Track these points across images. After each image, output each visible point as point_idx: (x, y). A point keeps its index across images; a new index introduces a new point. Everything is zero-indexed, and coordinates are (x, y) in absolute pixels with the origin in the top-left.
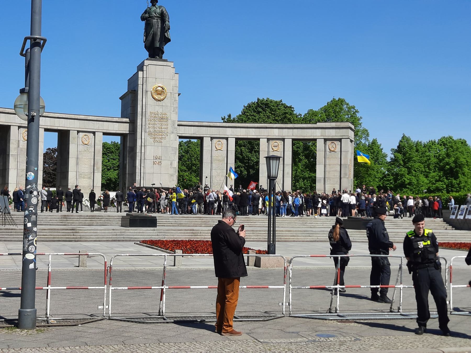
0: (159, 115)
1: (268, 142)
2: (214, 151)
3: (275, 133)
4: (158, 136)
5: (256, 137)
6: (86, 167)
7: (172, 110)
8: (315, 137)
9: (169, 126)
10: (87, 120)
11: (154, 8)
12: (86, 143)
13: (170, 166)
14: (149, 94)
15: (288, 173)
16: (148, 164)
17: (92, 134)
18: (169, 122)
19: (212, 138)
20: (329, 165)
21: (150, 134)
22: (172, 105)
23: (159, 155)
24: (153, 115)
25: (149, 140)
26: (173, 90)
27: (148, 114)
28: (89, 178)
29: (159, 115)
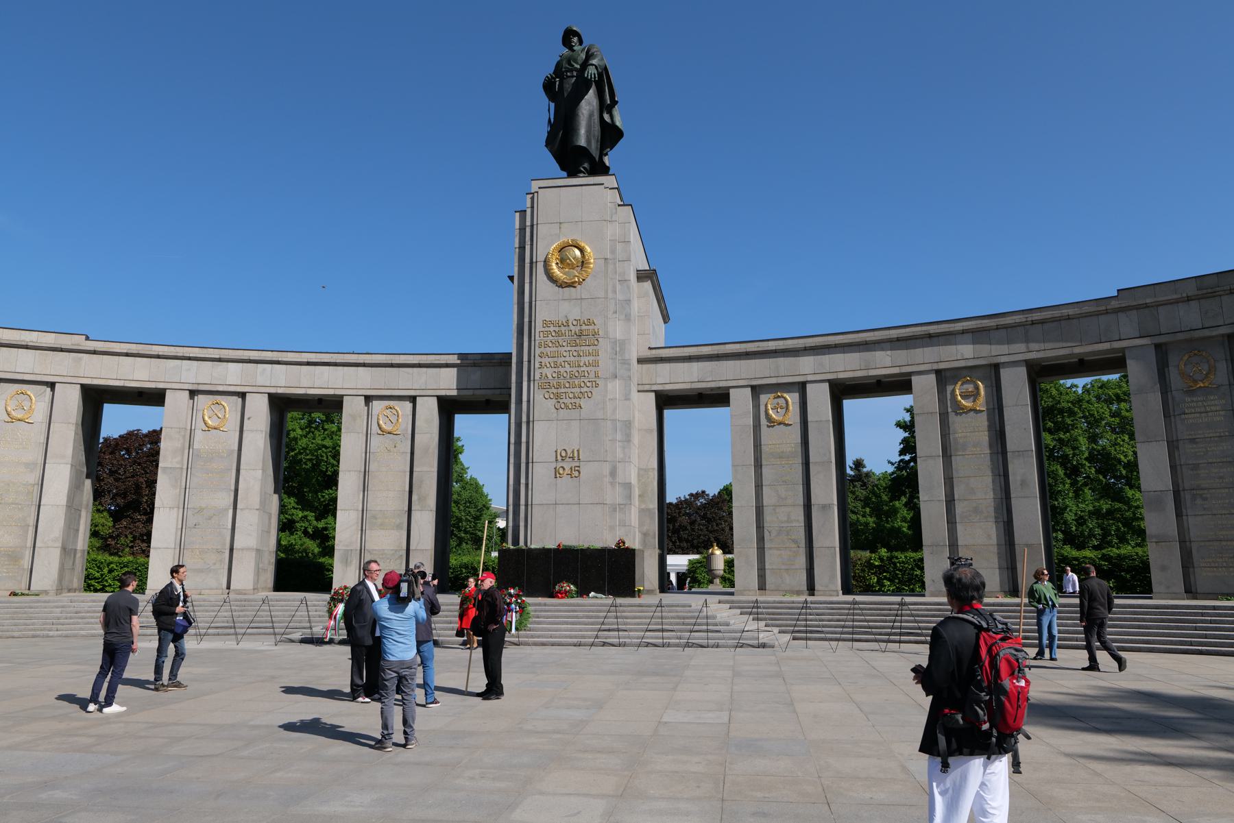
0: (572, 328)
2: (764, 429)
4: (573, 391)
5: (896, 371)
6: (388, 498)
9: (604, 358)
10: (392, 365)
13: (608, 479)
14: (540, 267)
15: (1024, 483)
16: (541, 474)
17: (409, 405)
18: (604, 347)
19: (756, 390)
20: (1193, 441)
21: (546, 386)
22: (610, 295)
23: (572, 444)
24: (552, 329)
25: (542, 404)
26: (613, 252)
27: (539, 326)
28: (398, 527)
29: (572, 328)
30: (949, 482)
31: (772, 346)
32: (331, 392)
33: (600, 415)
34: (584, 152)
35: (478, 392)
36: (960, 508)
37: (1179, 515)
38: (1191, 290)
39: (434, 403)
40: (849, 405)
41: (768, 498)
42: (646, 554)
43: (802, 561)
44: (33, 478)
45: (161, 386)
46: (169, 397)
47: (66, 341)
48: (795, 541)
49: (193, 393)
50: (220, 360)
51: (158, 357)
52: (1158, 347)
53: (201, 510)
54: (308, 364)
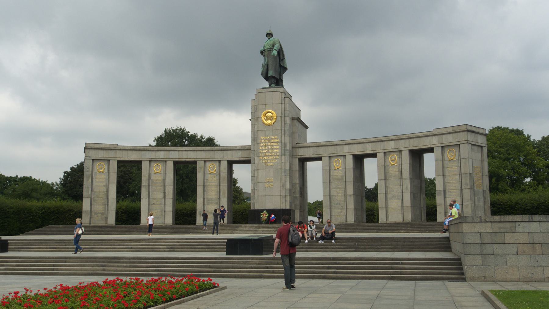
1: (384, 156)
3: (392, 145)
5: (372, 152)
7: (283, 132)
8: (432, 146)
10: (212, 150)
15: (407, 188)
17: (218, 163)
28: (216, 204)
30: (386, 187)
31: (335, 143)
32: (193, 160)
33: (279, 167)
34: (273, 77)
35: (241, 159)
36: (389, 196)
37: (445, 197)
38: (450, 130)
40: (366, 160)
41: (333, 192)
42: (296, 211)
43: (343, 213)
44: (105, 191)
45: (141, 159)
46: (143, 162)
47: (112, 147)
48: (342, 207)
49: (150, 161)
50: (158, 150)
51: (139, 150)
52: (442, 147)
53: (154, 199)
54: (186, 151)
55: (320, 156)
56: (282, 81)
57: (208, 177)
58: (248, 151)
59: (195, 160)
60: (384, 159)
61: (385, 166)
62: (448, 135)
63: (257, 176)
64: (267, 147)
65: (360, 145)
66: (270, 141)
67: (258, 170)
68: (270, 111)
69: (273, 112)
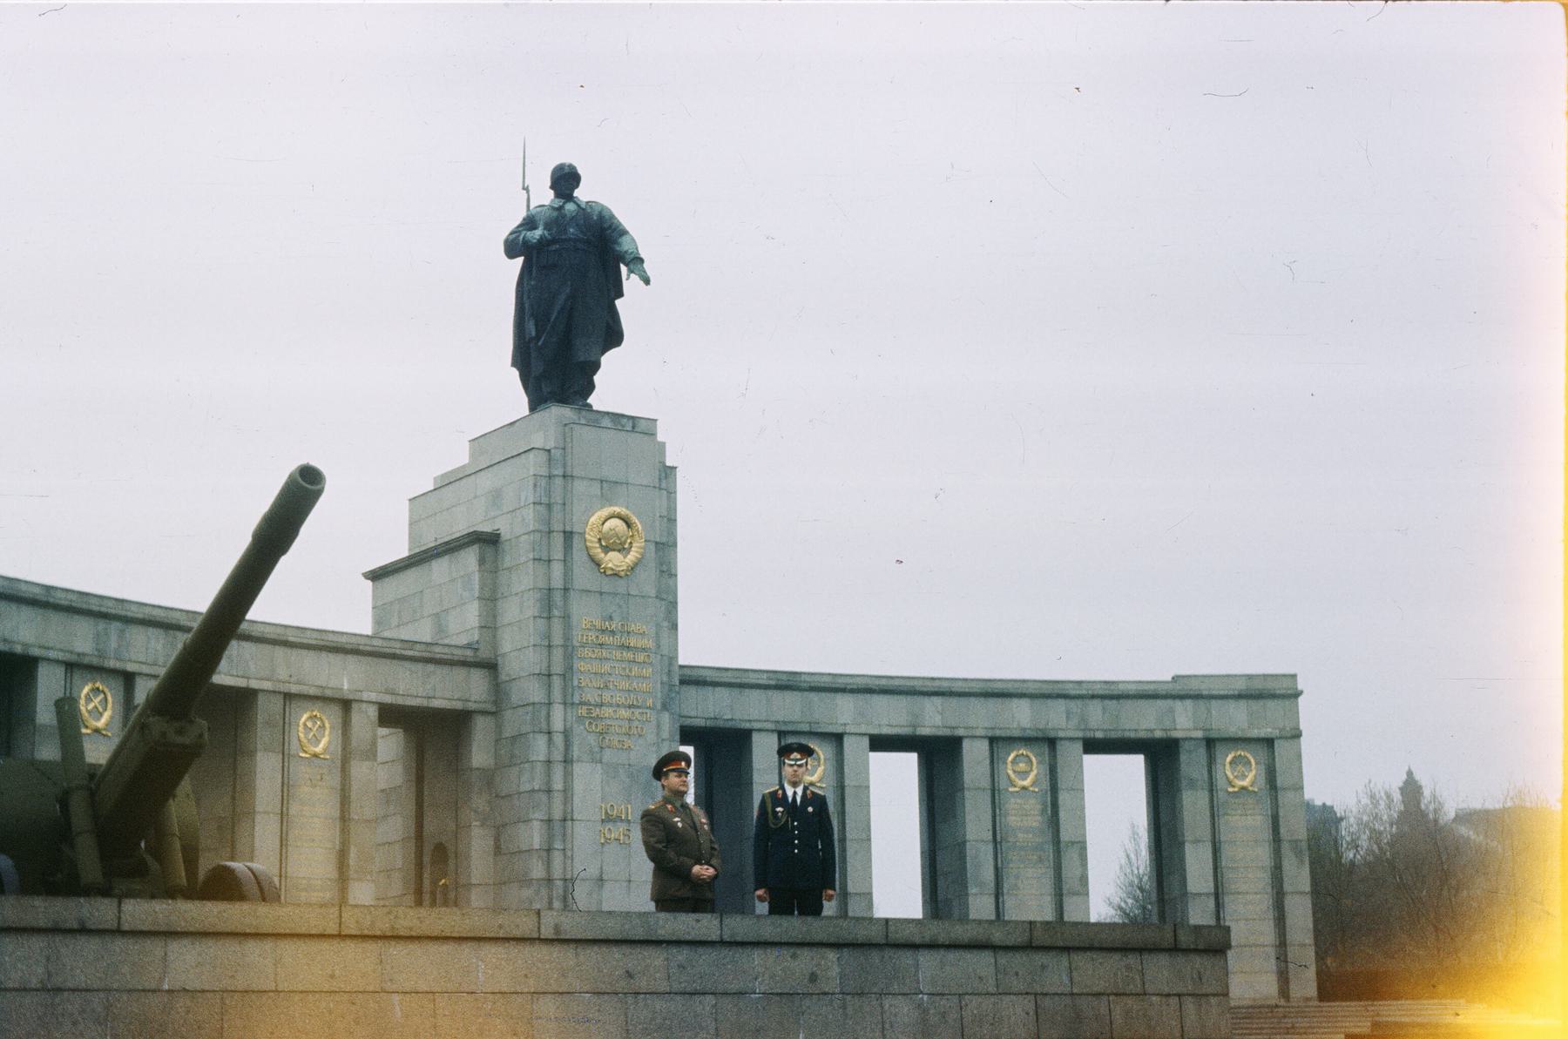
3: (1021, 716)
11: (570, 207)
12: (319, 749)
17: (335, 711)
32: (241, 683)
38: (1241, 686)
39: (373, 712)
51: (33, 603)
55: (747, 726)
56: (591, 387)
57: (301, 772)
58: (460, 673)
59: (254, 684)
60: (992, 762)
61: (993, 790)
62: (1232, 704)
63: (567, 792)
64: (606, 667)
65: (903, 701)
66: (617, 640)
67: (568, 761)
68: (623, 511)
69: (634, 519)
